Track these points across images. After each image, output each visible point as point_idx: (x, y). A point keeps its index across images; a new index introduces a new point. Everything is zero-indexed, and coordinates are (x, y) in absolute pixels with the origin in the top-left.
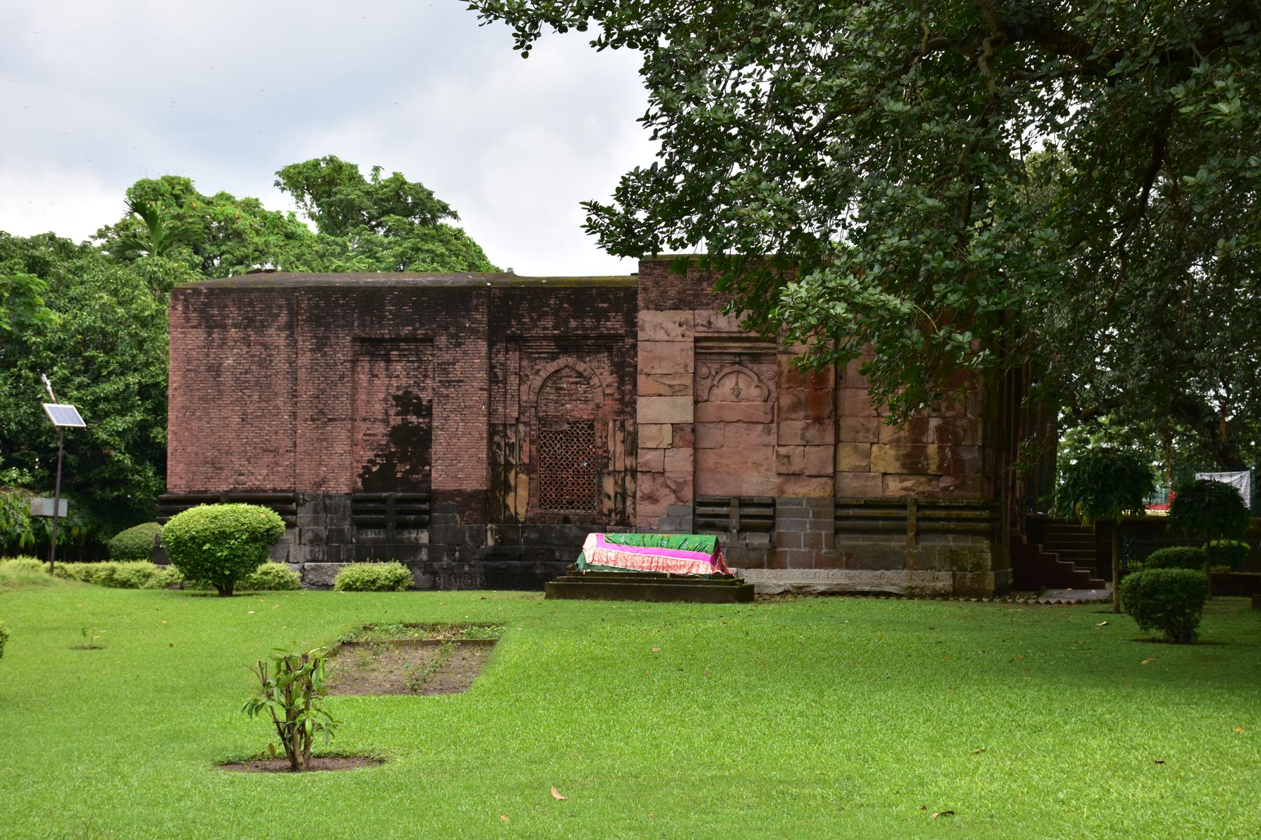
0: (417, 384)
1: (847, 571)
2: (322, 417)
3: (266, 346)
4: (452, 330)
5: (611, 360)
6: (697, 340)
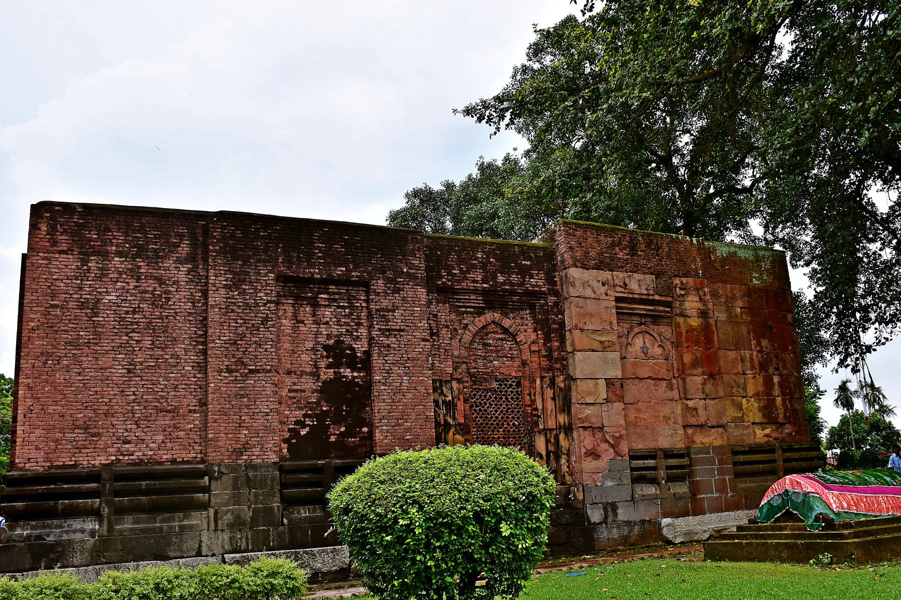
0: (349, 333)
2: (240, 368)
3: (160, 281)
4: (389, 274)
5: (534, 318)
6: (618, 300)
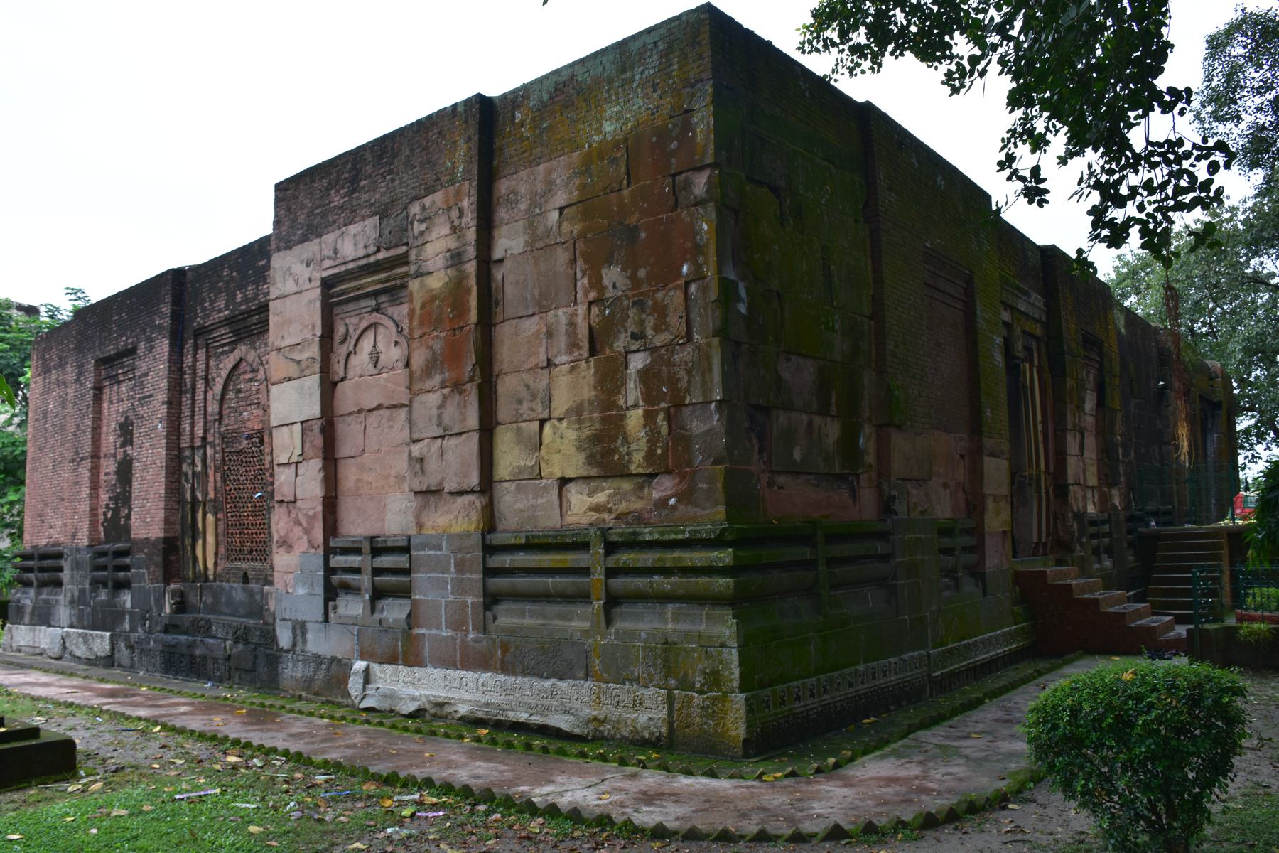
1: (502, 678)
